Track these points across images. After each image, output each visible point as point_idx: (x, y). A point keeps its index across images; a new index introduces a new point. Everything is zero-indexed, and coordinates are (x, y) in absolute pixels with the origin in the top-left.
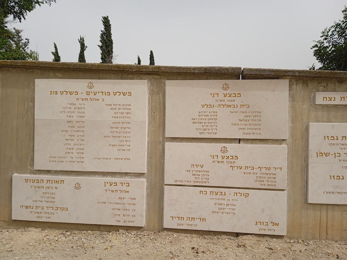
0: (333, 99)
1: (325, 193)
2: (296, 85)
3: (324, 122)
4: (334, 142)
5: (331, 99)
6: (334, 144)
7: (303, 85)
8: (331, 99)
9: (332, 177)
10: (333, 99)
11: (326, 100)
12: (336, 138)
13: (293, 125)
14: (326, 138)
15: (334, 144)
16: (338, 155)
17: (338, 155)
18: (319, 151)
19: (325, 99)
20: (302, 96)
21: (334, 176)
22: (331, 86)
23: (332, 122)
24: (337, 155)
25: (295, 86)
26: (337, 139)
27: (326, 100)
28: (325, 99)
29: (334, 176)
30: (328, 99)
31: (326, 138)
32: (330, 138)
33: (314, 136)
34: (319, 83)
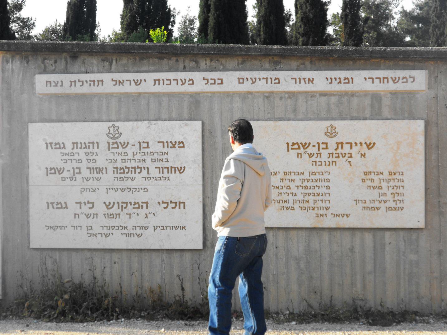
2: (12, 62)
7: (21, 62)
11: (164, 84)
13: (9, 126)
20: (20, 80)
25: (11, 65)
27: (164, 84)
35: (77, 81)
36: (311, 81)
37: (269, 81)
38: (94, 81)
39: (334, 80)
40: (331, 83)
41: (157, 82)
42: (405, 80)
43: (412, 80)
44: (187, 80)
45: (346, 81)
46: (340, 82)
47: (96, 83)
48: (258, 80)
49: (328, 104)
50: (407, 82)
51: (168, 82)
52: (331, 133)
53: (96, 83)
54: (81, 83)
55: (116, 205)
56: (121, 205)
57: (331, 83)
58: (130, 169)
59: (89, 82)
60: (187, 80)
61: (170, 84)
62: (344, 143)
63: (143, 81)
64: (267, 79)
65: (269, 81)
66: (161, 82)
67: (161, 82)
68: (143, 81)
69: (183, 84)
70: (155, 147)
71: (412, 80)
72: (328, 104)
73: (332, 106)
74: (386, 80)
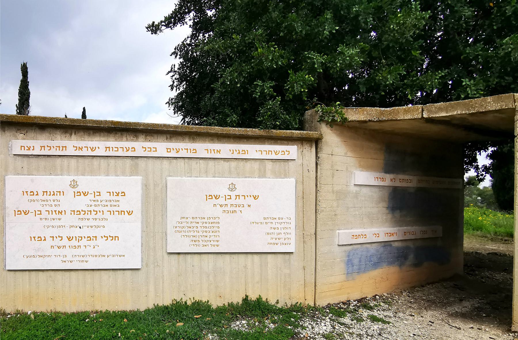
0: (32, 148)
1: (25, 257)
3: (25, 175)
4: (35, 197)
5: (29, 149)
6: (34, 201)
8: (29, 149)
9: (33, 239)
10: (32, 148)
12: (36, 193)
14: (25, 193)
15: (34, 201)
16: (39, 213)
17: (39, 213)
18: (17, 208)
19: (23, 148)
21: (34, 237)
22: (31, 134)
23: (33, 175)
24: (38, 212)
26: (37, 194)
28: (23, 148)
29: (34, 237)
30: (26, 148)
31: (25, 193)
32: (29, 193)
33: (11, 191)
34: (18, 130)
35: (46, 146)
36: (219, 151)
37: (189, 151)
38: (59, 147)
39: (235, 151)
40: (233, 153)
41: (108, 149)
42: (283, 153)
43: (288, 153)
44: (130, 148)
45: (244, 152)
46: (239, 153)
47: (61, 148)
48: (181, 150)
49: (230, 168)
50: (284, 154)
51: (116, 149)
52: (232, 188)
53: (61, 148)
54: (49, 148)
55: (74, 238)
56: (77, 238)
57: (233, 153)
58: (87, 212)
59: (55, 148)
60: (130, 148)
61: (118, 151)
62: (241, 195)
63: (97, 148)
64: (187, 149)
65: (189, 151)
66: (111, 149)
67: (111, 149)
68: (97, 148)
69: (127, 151)
70: (105, 196)
71: (288, 153)
72: (230, 168)
73: (233, 169)
74: (270, 152)
